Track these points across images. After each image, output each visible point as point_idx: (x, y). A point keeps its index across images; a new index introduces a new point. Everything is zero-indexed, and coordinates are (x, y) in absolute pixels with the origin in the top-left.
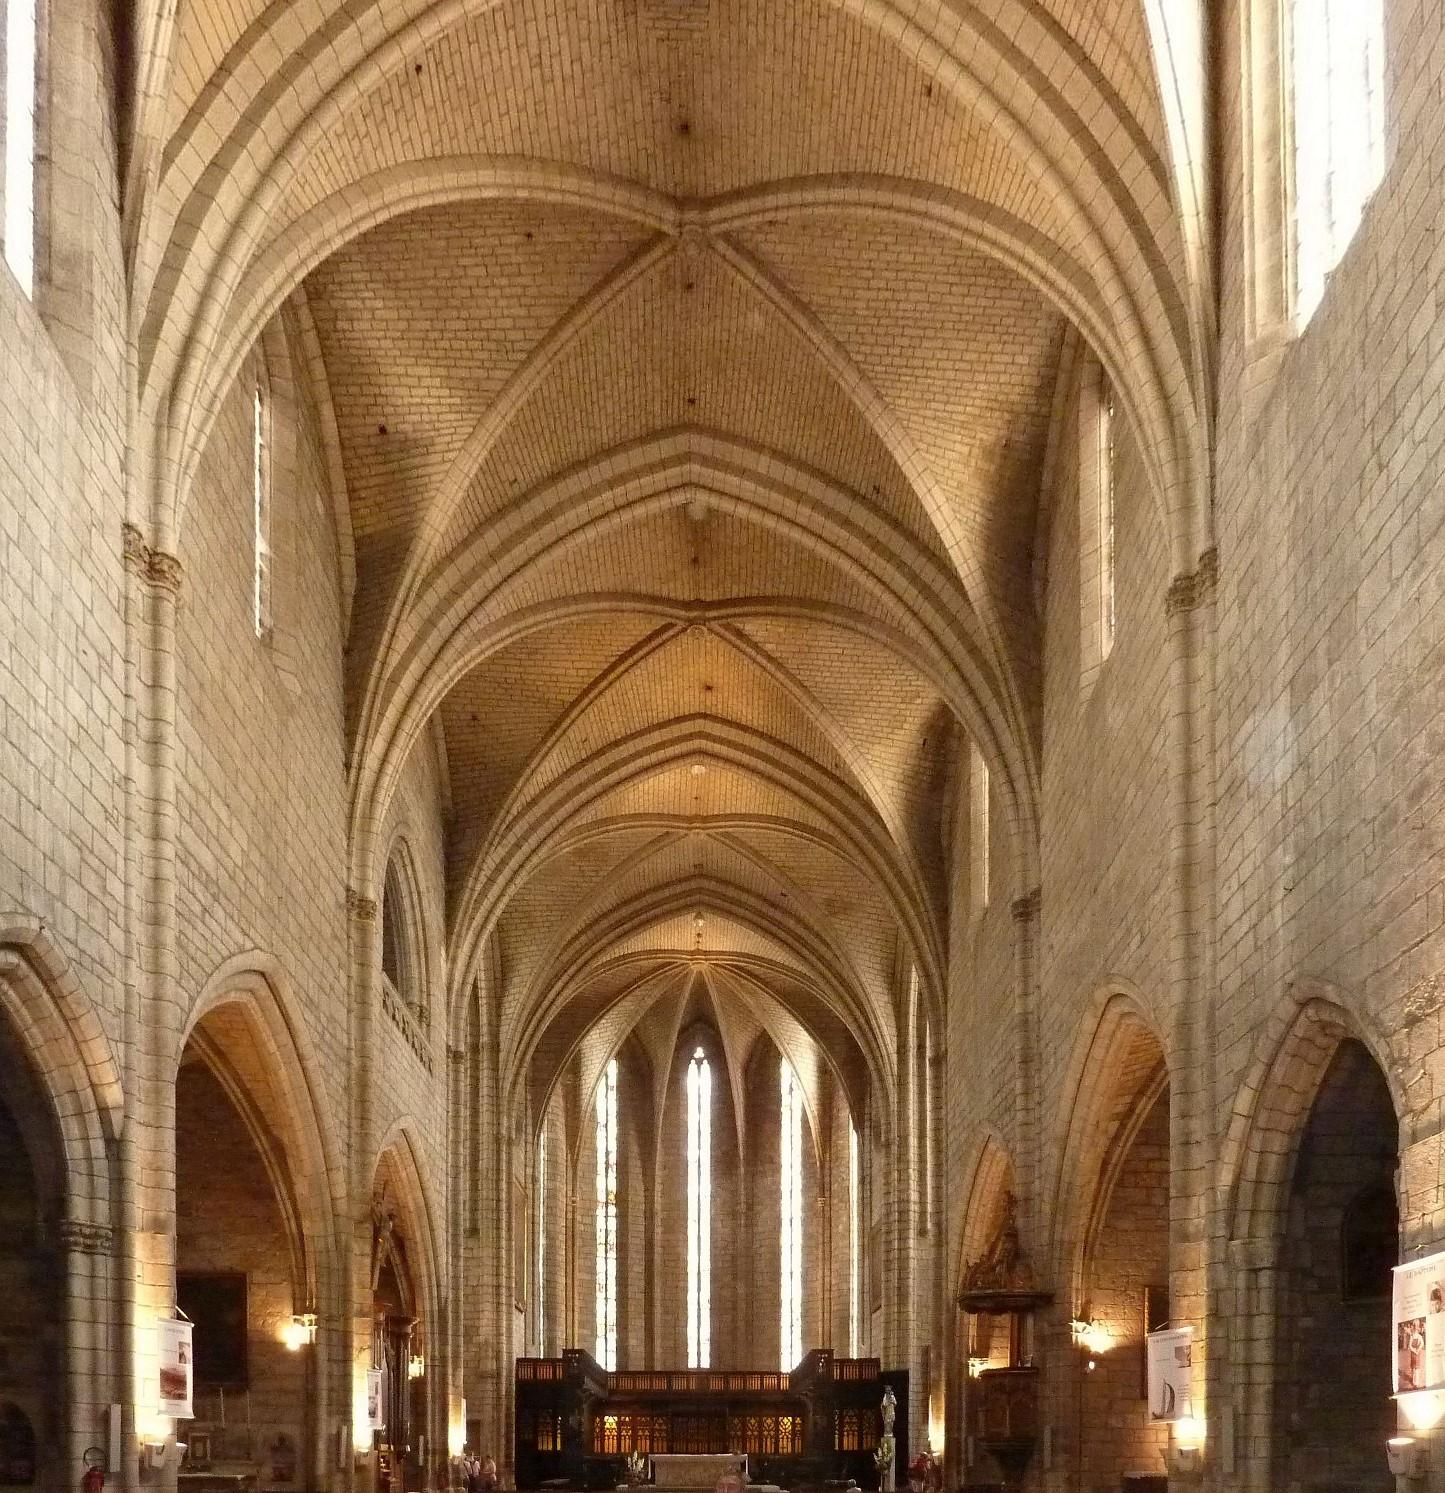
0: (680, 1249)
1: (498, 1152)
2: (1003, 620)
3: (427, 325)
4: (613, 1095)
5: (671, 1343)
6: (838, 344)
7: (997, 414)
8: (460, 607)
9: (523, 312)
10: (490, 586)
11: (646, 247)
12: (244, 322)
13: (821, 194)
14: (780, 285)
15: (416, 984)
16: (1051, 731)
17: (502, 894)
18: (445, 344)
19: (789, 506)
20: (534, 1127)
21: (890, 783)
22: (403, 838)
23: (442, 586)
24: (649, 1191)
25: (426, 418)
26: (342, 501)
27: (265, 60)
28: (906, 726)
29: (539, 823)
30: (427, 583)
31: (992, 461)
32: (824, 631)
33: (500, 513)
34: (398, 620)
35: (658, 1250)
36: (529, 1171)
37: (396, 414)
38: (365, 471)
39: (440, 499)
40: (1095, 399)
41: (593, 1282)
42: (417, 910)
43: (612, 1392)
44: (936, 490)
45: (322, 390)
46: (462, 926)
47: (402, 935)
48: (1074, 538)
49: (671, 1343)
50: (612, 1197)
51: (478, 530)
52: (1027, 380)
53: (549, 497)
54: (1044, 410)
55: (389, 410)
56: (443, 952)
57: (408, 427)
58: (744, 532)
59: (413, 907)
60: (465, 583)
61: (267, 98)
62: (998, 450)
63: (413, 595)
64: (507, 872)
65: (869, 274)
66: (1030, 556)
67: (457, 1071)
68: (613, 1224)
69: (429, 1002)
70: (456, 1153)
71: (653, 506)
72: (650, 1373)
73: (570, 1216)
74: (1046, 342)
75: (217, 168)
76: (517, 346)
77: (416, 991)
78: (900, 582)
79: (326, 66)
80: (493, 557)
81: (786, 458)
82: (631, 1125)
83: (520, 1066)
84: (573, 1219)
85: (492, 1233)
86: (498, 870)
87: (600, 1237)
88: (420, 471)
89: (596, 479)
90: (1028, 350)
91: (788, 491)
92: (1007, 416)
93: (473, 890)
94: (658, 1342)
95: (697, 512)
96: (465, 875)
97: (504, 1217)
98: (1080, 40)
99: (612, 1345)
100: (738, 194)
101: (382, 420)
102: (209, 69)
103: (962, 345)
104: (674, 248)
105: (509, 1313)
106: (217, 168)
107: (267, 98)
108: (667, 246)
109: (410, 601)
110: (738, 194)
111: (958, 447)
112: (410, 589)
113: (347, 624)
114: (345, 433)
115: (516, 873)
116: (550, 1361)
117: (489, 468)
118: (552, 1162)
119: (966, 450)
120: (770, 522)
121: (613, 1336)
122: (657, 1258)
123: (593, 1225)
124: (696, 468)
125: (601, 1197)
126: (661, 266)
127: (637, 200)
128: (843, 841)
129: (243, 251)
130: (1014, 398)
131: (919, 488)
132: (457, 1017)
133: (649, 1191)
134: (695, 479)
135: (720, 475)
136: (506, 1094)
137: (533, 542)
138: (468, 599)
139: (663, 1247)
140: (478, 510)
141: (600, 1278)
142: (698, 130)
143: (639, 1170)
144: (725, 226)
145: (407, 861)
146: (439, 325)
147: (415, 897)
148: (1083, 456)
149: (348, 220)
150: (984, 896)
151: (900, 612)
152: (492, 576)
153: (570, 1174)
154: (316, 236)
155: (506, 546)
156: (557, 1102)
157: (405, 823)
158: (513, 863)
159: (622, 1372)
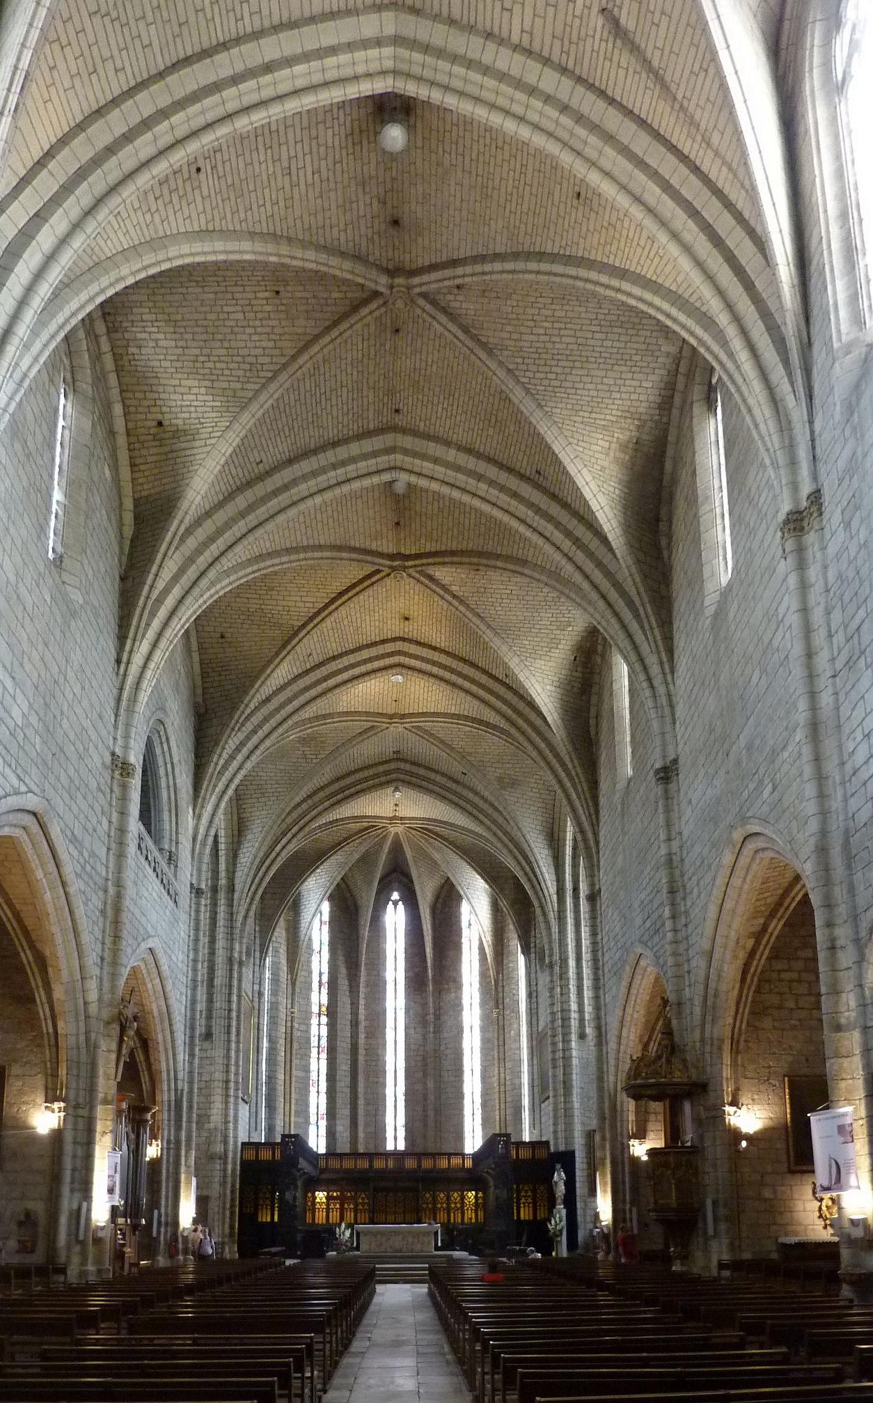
0: (380, 1052)
1: (231, 970)
2: (638, 562)
3: (197, 352)
4: (326, 928)
7: (629, 421)
8: (214, 549)
9: (271, 344)
10: (239, 535)
11: (366, 302)
12: (53, 327)
13: (498, 266)
14: (466, 330)
15: (167, 834)
16: (680, 642)
18: (210, 365)
19: (472, 483)
20: (261, 952)
23: (201, 534)
24: (354, 1005)
25: (193, 415)
26: (125, 472)
27: (81, 150)
30: (189, 532)
32: (495, 576)
33: (249, 484)
34: (165, 555)
35: (361, 1051)
36: (256, 987)
37: (170, 413)
38: (144, 452)
39: (202, 471)
40: (705, 409)
42: (171, 777)
43: (323, 1171)
44: (585, 472)
45: (115, 393)
47: (157, 797)
48: (693, 501)
49: (372, 1129)
50: (324, 1009)
51: (230, 497)
52: (652, 398)
53: (286, 475)
54: (665, 419)
55: (164, 409)
56: (191, 810)
57: (180, 422)
58: (436, 504)
59: (167, 775)
60: (219, 532)
61: (81, 175)
62: (631, 445)
63: (177, 538)
65: (531, 324)
66: (658, 520)
67: (198, 904)
68: (324, 1031)
69: (177, 848)
71: (367, 482)
72: (355, 1155)
74: (664, 372)
75: (39, 218)
76: (265, 367)
77: (166, 840)
78: (558, 536)
79: (127, 158)
80: (242, 515)
81: (469, 451)
82: (340, 952)
84: (292, 1027)
85: (224, 1037)
87: (314, 1041)
88: (188, 452)
89: (323, 463)
90: (651, 377)
91: (471, 473)
92: (636, 422)
94: (361, 1128)
95: (400, 488)
97: (234, 1023)
98: (692, 157)
99: (323, 1131)
100: (433, 267)
101: (160, 417)
102: (37, 154)
103: (602, 373)
104: (385, 303)
105: (236, 1104)
106: (39, 218)
107: (81, 175)
108: (381, 302)
109: (175, 543)
110: (433, 267)
111: (600, 442)
112: (175, 534)
113: (125, 559)
114: (131, 425)
116: (270, 1145)
117: (240, 451)
118: (275, 980)
119: (606, 445)
120: (456, 494)
121: (323, 1123)
122: (361, 1058)
123: (308, 1031)
124: (399, 457)
125: (315, 1009)
126: (377, 313)
127: (359, 268)
129: (55, 275)
130: (641, 410)
131: (572, 470)
132: (200, 862)
133: (354, 1005)
134: (399, 464)
135: (417, 462)
136: (239, 924)
137: (274, 504)
138: (221, 543)
141: (313, 1076)
142: (405, 220)
144: (424, 289)
145: (164, 739)
146: (205, 351)
147: (169, 766)
148: (697, 447)
149: (139, 266)
150: (627, 768)
151: (557, 556)
152: (240, 527)
154: (113, 275)
155: (251, 508)
156: (280, 934)
157: (163, 709)
159: (331, 1154)
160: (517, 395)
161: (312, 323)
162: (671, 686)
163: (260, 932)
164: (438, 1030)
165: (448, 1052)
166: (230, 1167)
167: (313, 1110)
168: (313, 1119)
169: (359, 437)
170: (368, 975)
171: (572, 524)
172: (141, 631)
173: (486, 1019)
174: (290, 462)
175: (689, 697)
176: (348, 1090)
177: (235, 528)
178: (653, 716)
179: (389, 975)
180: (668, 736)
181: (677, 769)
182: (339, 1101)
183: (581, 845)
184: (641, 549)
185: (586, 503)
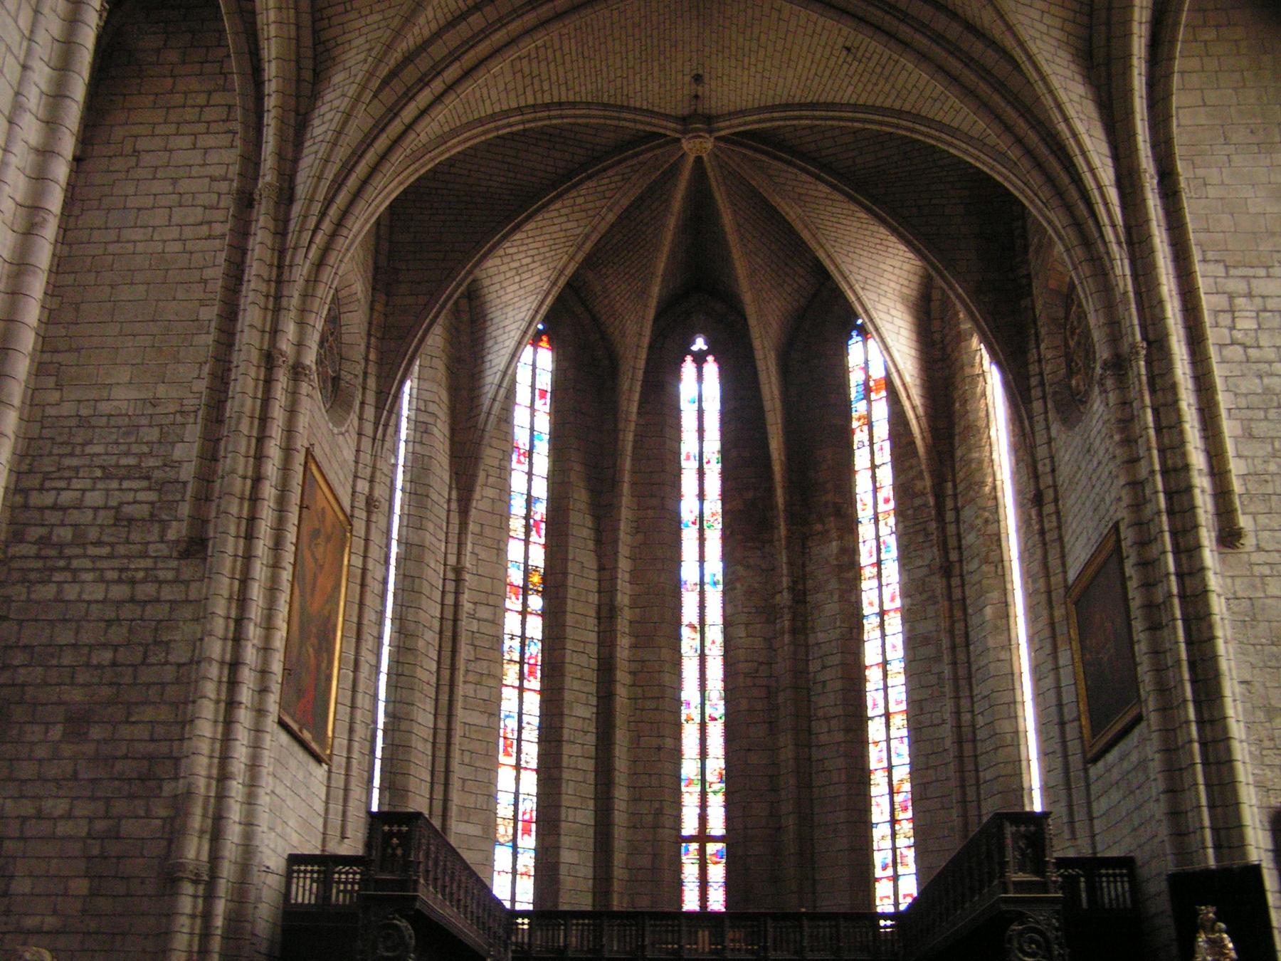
1: (269, 382)
5: (645, 861)
24: (606, 570)
36: (363, 486)
41: (492, 729)
49: (645, 861)
50: (536, 579)
68: (535, 627)
73: (450, 599)
84: (457, 605)
87: (511, 647)
94: (619, 858)
99: (527, 861)
121: (528, 842)
125: (516, 576)
133: (606, 570)
139: (633, 673)
153: (455, 528)
164: (801, 626)
165: (827, 675)
166: (220, 907)
167: (504, 808)
168: (504, 831)
173: (912, 589)
176: (590, 765)
179: (688, 508)
182: (568, 789)
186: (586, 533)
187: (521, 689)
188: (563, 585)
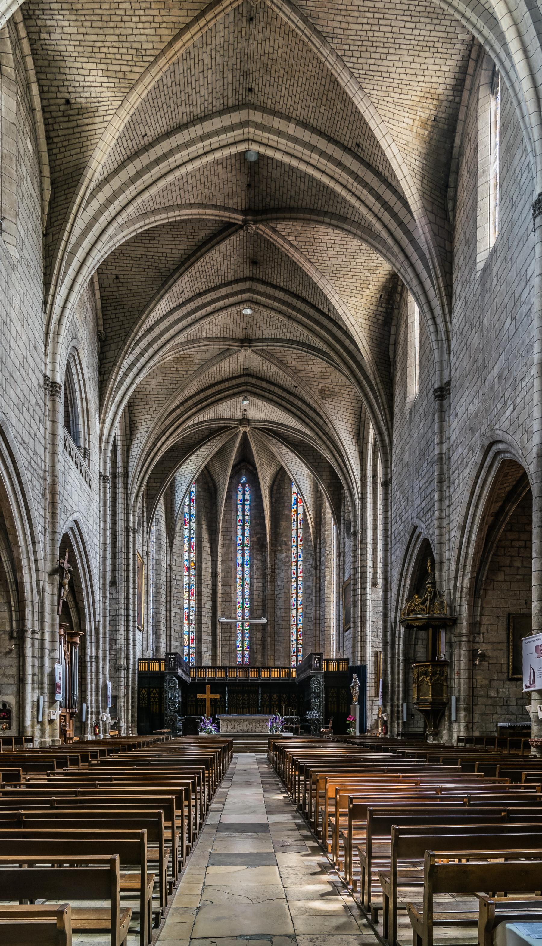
1: (128, 536)
2: (430, 222)
3: (94, 38)
6: (338, 56)
7: (429, 101)
8: (112, 210)
9: (152, 31)
10: (130, 197)
14: (305, 20)
15: (82, 435)
17: (132, 383)
18: (105, 50)
20: (148, 522)
21: (360, 320)
22: (75, 348)
23: (102, 197)
25: (93, 95)
28: (370, 287)
29: (155, 340)
30: (93, 195)
31: (425, 129)
32: (324, 229)
33: (136, 154)
34: (76, 216)
35: (219, 595)
36: (145, 548)
37: (75, 92)
39: (101, 145)
40: (489, 92)
42: (83, 391)
44: (393, 146)
46: (108, 401)
47: (74, 406)
48: (474, 173)
50: (192, 564)
51: (122, 165)
53: (165, 146)
54: (457, 99)
55: (71, 89)
57: (83, 100)
58: (278, 169)
59: (80, 390)
60: (115, 196)
62: (429, 122)
63: (85, 201)
64: (135, 370)
65: (356, 14)
66: (447, 186)
69: (89, 445)
70: (105, 536)
71: (227, 152)
73: (168, 575)
74: (459, 58)
76: (148, 52)
77: (81, 440)
78: (371, 200)
80: (132, 180)
81: (305, 125)
83: (140, 486)
84: (170, 577)
86: (130, 368)
88: (90, 127)
89: (193, 136)
90: (449, 62)
92: (435, 102)
93: (115, 380)
94: (219, 650)
95: (253, 158)
96: (110, 371)
101: (67, 95)
103: (410, 59)
109: (83, 205)
111: (406, 120)
112: (83, 198)
113: (45, 218)
115: (140, 370)
117: (130, 127)
118: (158, 543)
119: (411, 122)
120: (295, 163)
122: (219, 600)
124: (252, 130)
128: (332, 354)
130: (440, 91)
131: (383, 144)
132: (105, 456)
134: (251, 136)
135: (266, 135)
136: (132, 502)
137: (156, 172)
138: (117, 205)
140: (124, 153)
143: (208, 549)
145: (77, 362)
146: (102, 38)
147: (82, 382)
148: (480, 126)
151: (370, 217)
152: (131, 191)
153: (168, 552)
155: (139, 174)
156: (161, 509)
157: (76, 338)
158: (139, 365)
160: (344, 78)
161: (184, 13)
162: (449, 324)
163: (147, 507)
169: (220, 113)
170: (224, 539)
171: (382, 189)
172: (61, 277)
174: (168, 134)
175: (461, 334)
176: (210, 622)
177: (127, 192)
178: (435, 347)
180: (445, 363)
181: (449, 389)
183: (379, 445)
184: (432, 212)
185: (393, 173)
186: (208, 549)
187: (189, 600)
188: (201, 567)
